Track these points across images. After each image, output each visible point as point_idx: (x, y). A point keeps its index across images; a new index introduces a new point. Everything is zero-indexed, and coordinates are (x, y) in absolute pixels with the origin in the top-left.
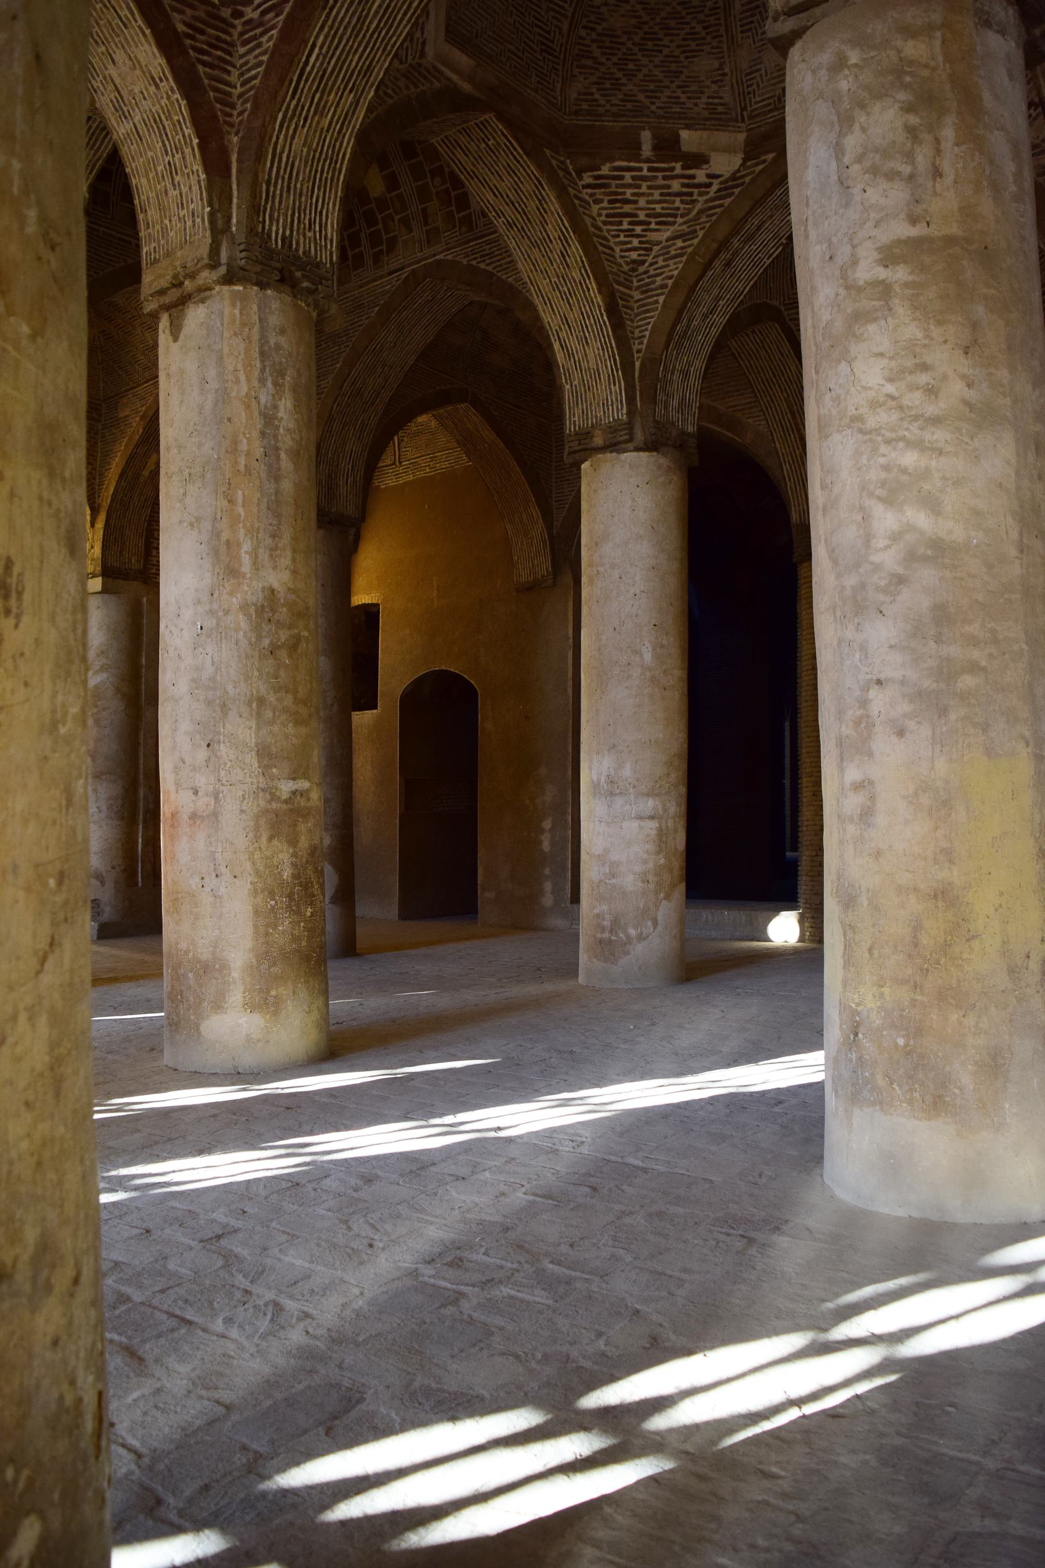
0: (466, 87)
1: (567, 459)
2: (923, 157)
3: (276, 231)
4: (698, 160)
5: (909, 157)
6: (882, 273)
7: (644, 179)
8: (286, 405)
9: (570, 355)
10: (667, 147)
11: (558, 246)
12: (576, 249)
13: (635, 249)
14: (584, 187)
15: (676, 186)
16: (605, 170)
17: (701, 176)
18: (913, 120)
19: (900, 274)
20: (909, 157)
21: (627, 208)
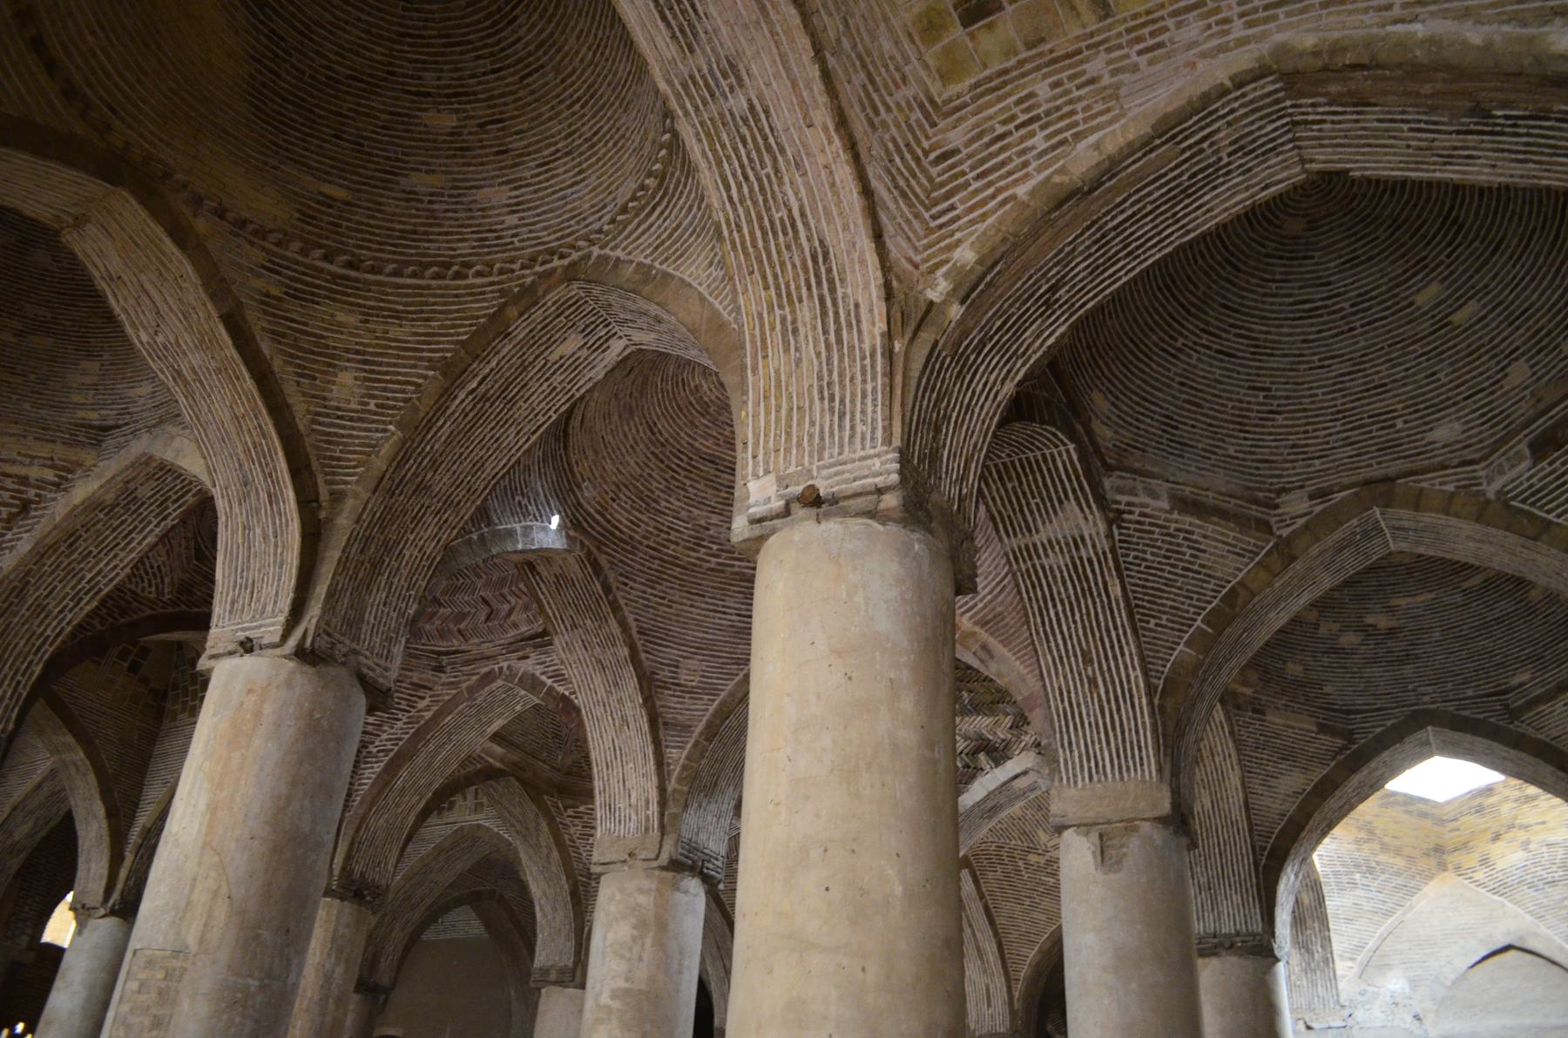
0: (498, 765)
1: (532, 985)
2: (636, 951)
3: (358, 869)
5: (630, 949)
6: (610, 1002)
8: (339, 970)
9: (545, 916)
11: (545, 850)
12: (555, 854)
16: (582, 809)
18: (635, 933)
19: (617, 1004)
20: (630, 949)
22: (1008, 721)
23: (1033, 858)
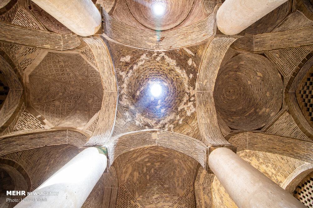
4: (44, 124)
7: (33, 120)
10: (41, 119)
13: (19, 128)
14: (23, 114)
15: (37, 124)
16: (29, 114)
17: (42, 126)
21: (26, 122)
22: (155, 122)
23: (132, 202)
